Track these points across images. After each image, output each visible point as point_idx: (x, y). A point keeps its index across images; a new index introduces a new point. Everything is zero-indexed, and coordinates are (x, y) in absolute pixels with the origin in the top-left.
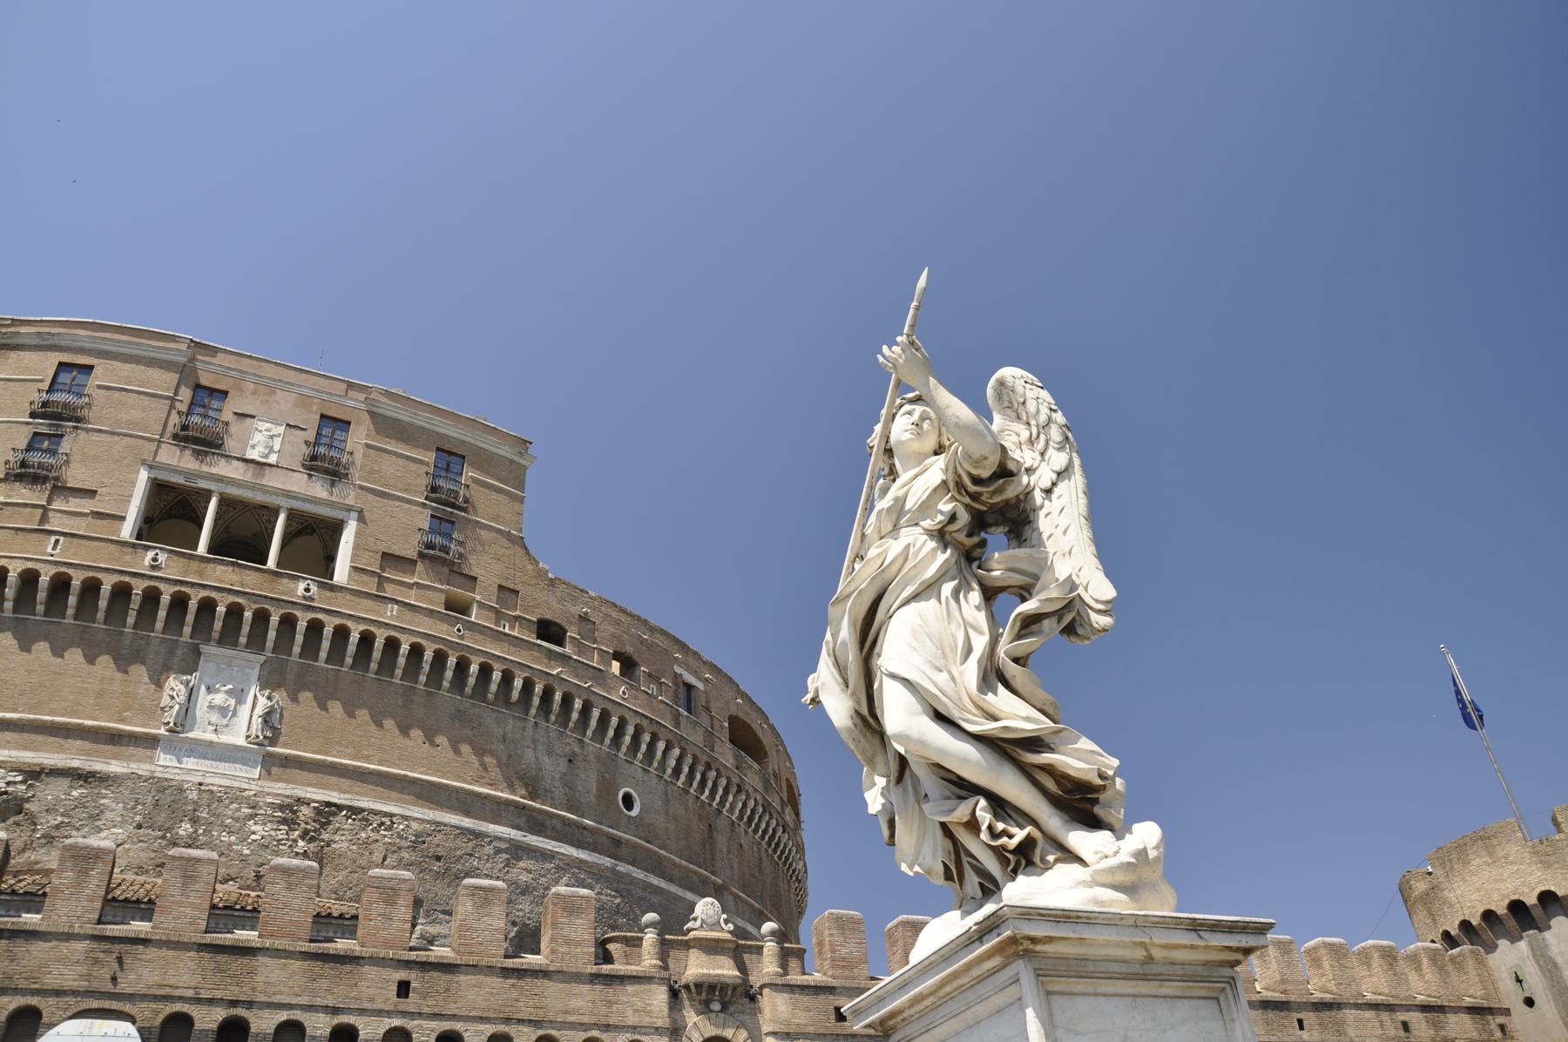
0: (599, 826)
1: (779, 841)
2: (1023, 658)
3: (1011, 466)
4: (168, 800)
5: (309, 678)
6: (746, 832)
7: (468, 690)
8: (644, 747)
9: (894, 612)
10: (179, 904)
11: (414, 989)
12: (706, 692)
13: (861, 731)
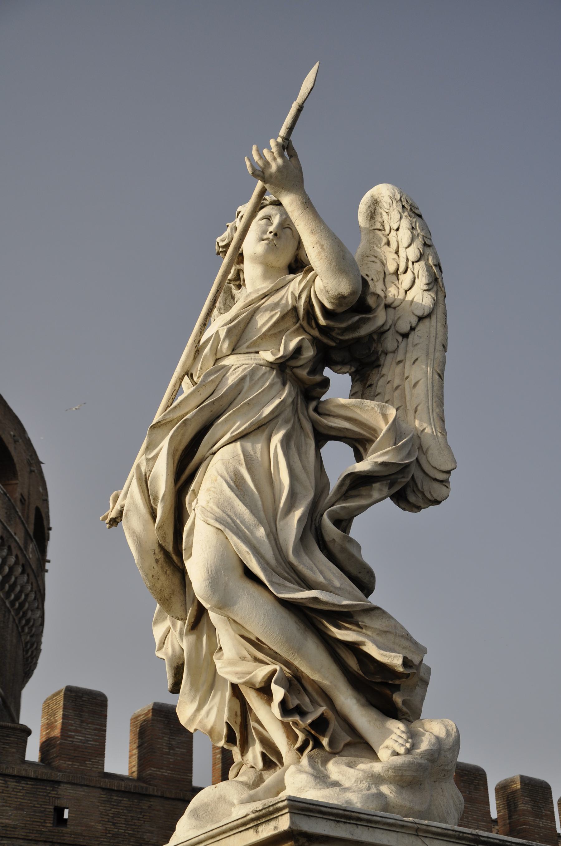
2: (346, 520)
3: (371, 301)
9: (218, 450)
13: (162, 567)
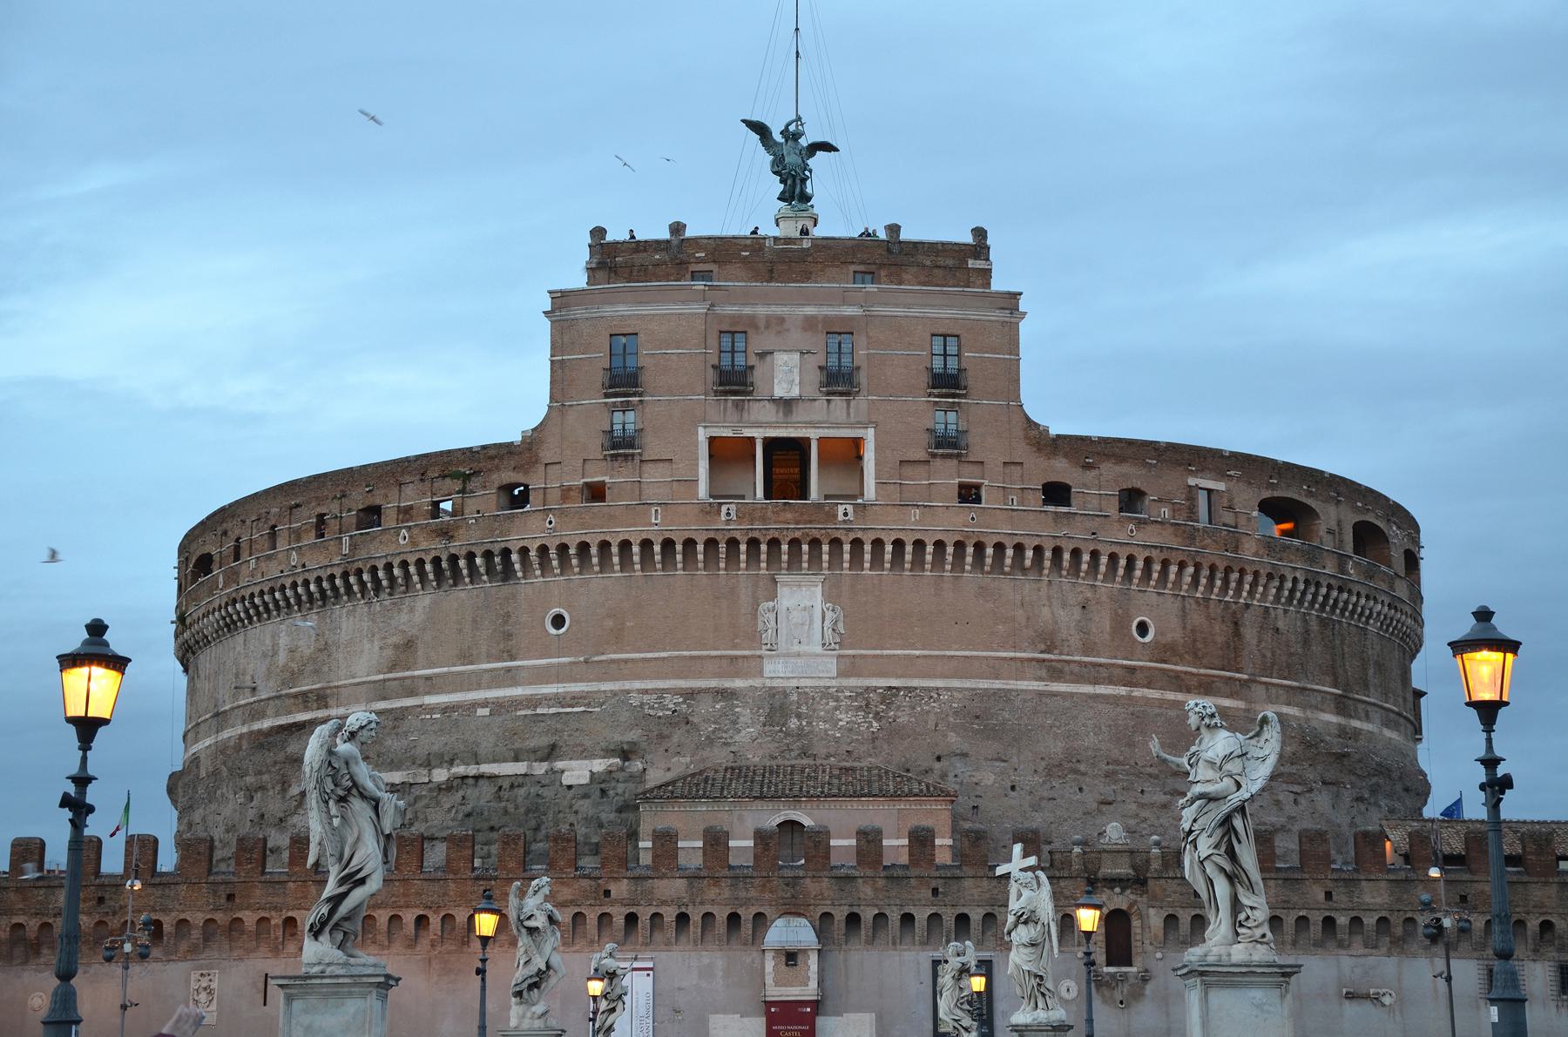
0: (1114, 661)
1: (1336, 601)
4: (778, 703)
5: (859, 587)
6: (1286, 611)
7: (987, 568)
8: (1155, 575)
10: (814, 857)
11: (942, 893)
12: (1228, 490)
